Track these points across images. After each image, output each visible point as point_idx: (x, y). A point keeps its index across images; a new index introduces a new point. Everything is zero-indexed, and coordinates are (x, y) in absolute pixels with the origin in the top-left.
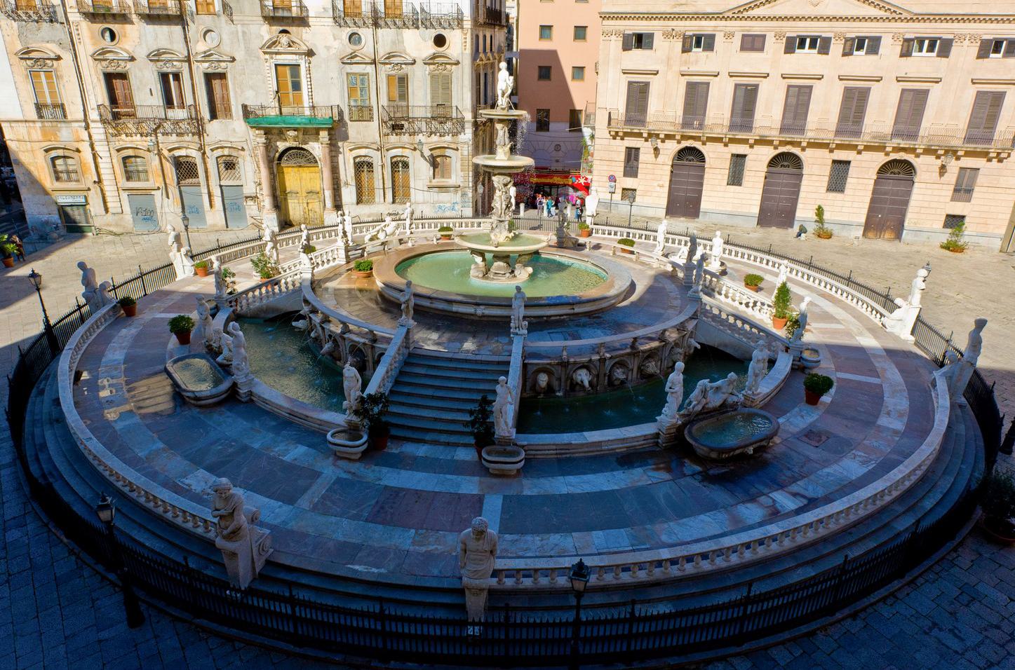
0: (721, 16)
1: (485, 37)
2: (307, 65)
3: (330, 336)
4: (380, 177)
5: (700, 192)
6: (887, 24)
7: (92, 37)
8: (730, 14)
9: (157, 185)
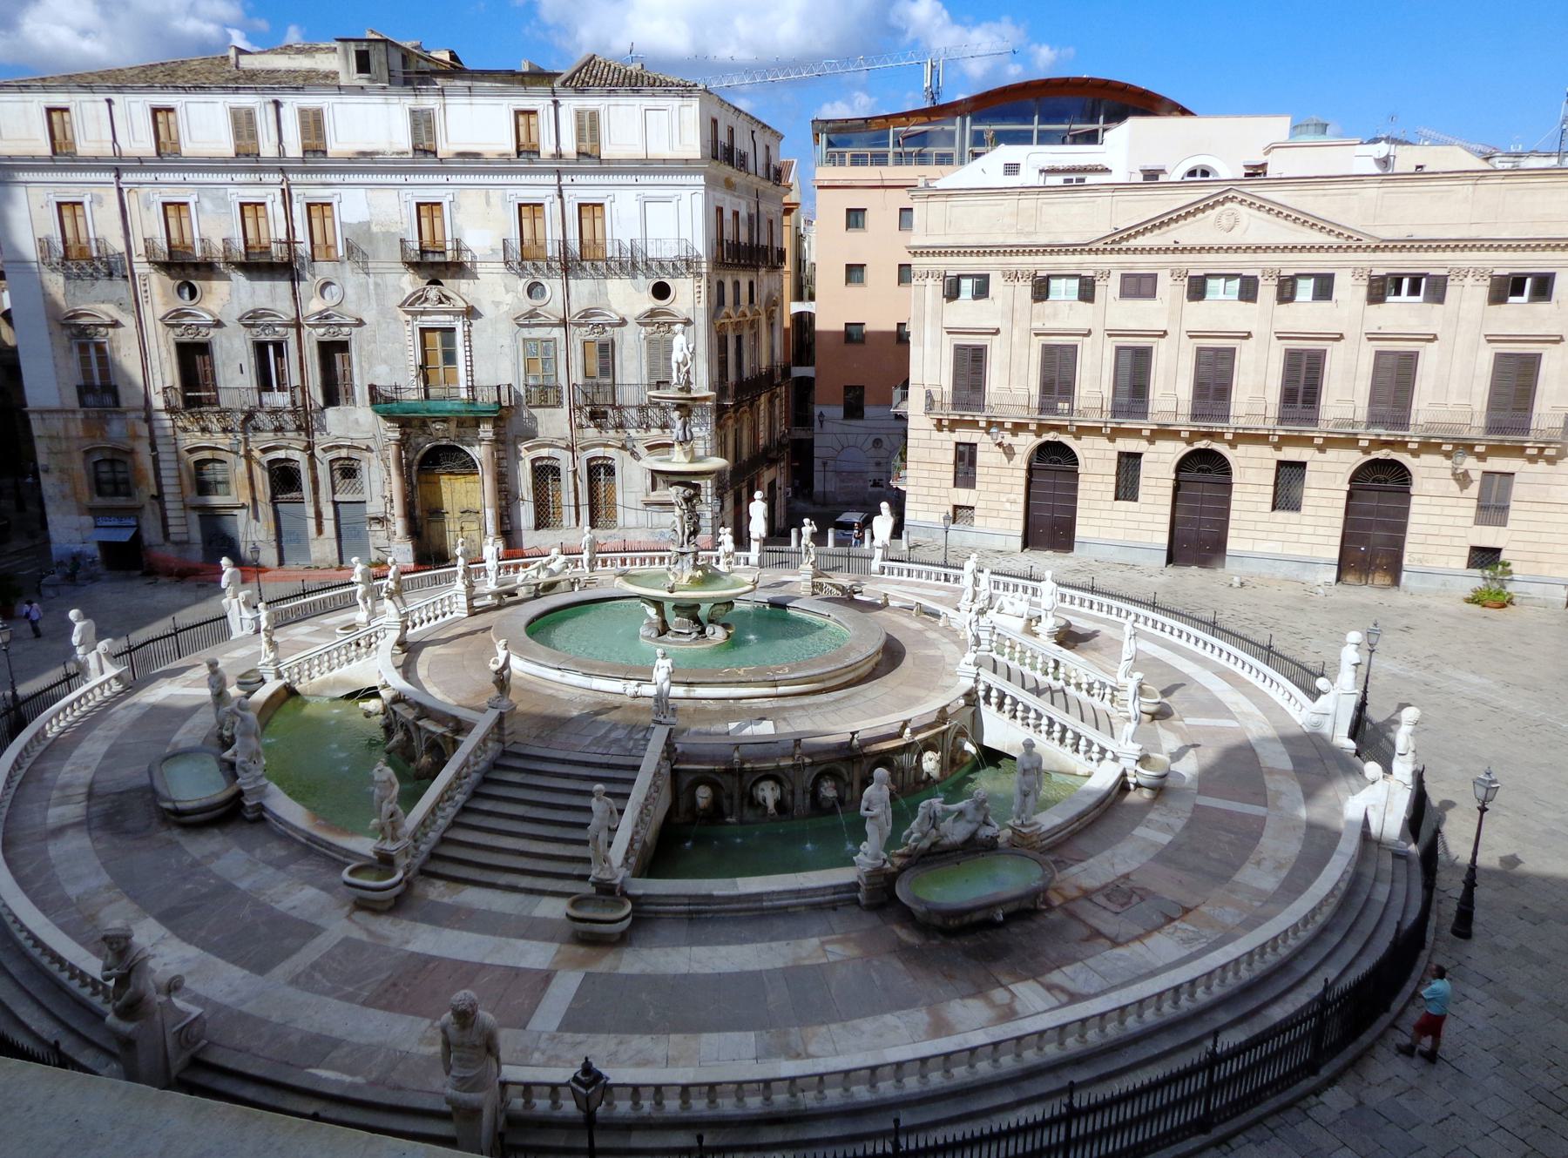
0: (1087, 248)
1: (737, 284)
3: (402, 725)
4: (571, 488)
5: (1073, 511)
6: (1341, 256)
7: (165, 295)
8: (1100, 245)
9: (242, 501)
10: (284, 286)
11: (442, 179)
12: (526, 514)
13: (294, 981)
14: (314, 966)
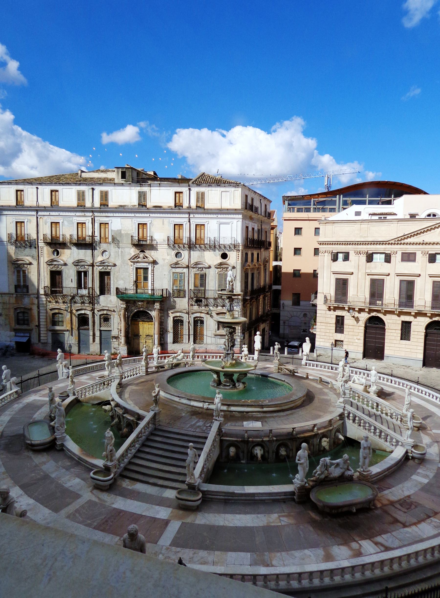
0: (388, 243)
1: (252, 254)
2: (152, 268)
4: (187, 328)
5: (383, 344)
8: (393, 242)
9: (67, 328)
10: (89, 252)
11: (147, 215)
12: (170, 337)
13: (68, 517)
14: (77, 511)
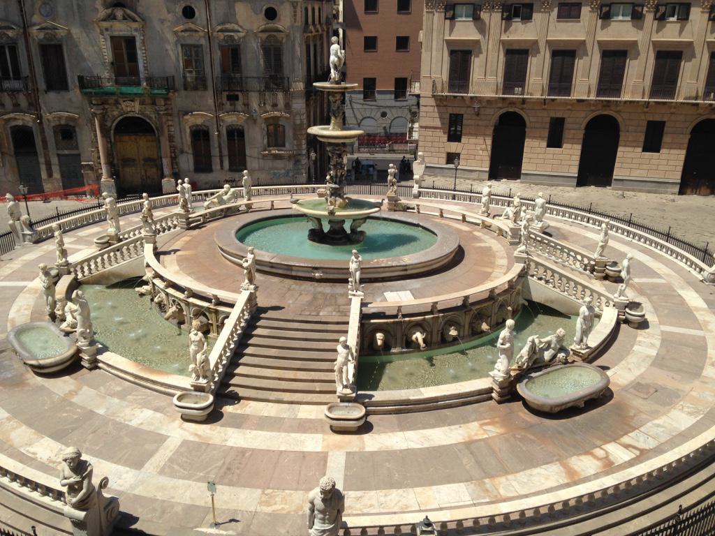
1: (313, 9)
3: (174, 301)
13: (162, 472)
14: (171, 460)
